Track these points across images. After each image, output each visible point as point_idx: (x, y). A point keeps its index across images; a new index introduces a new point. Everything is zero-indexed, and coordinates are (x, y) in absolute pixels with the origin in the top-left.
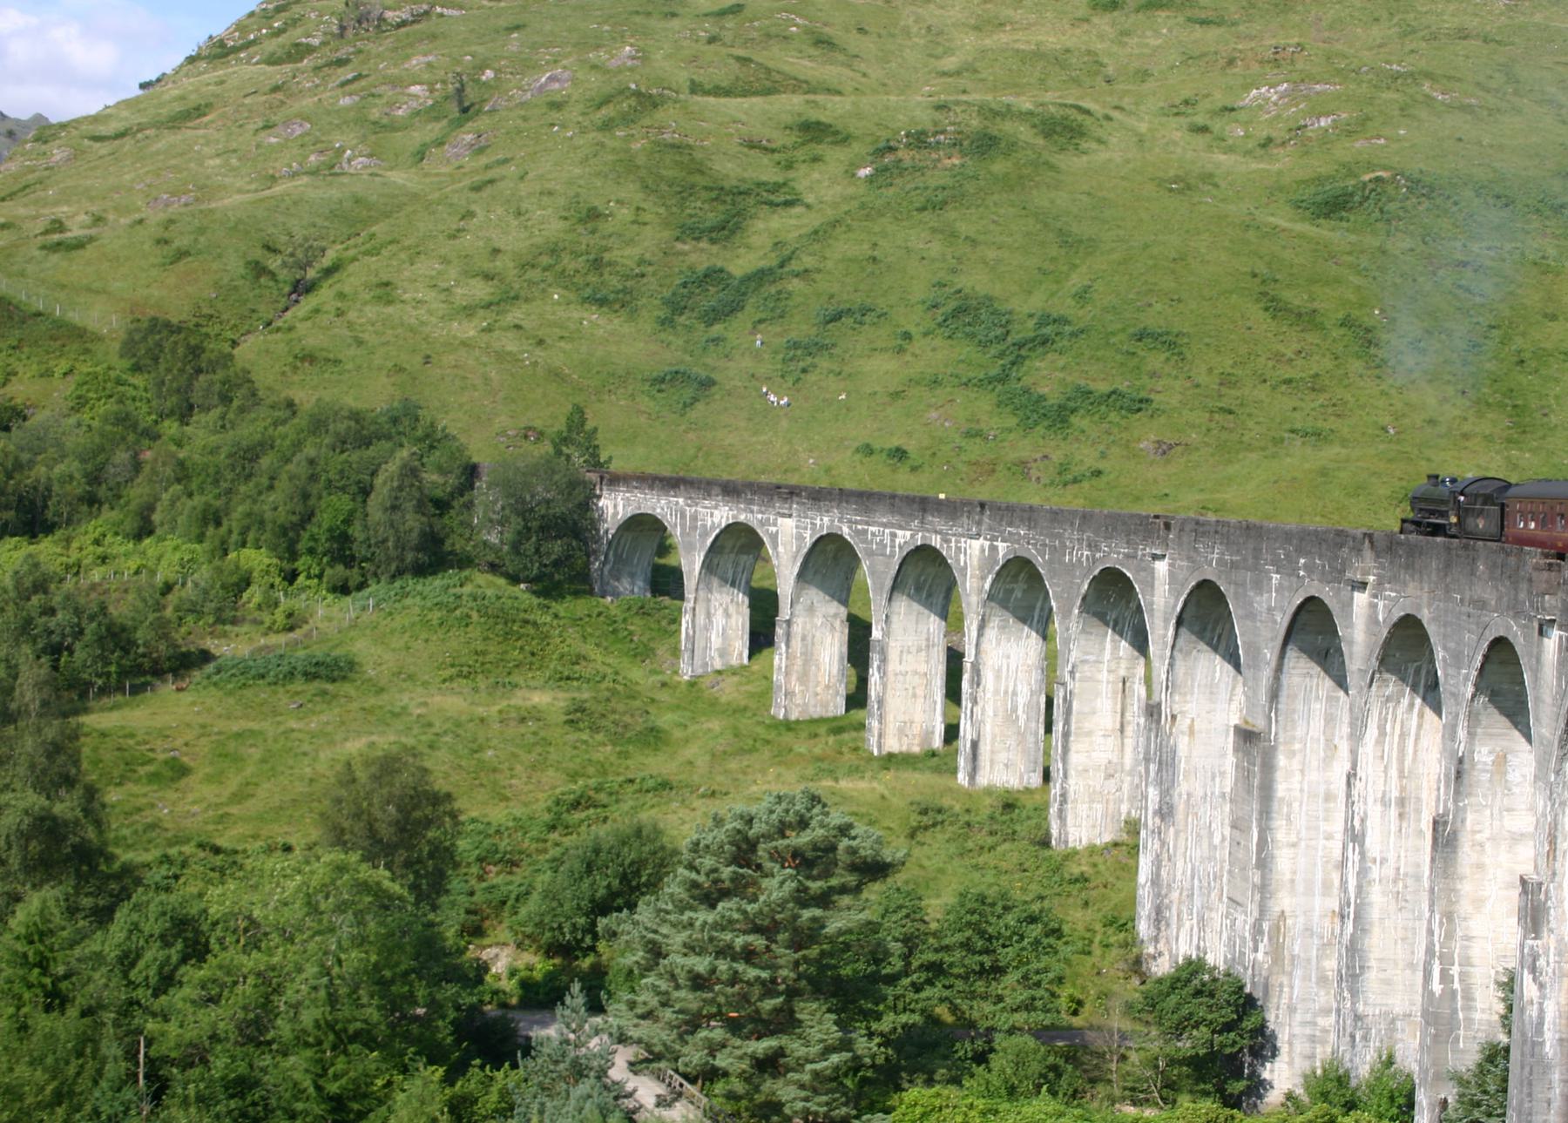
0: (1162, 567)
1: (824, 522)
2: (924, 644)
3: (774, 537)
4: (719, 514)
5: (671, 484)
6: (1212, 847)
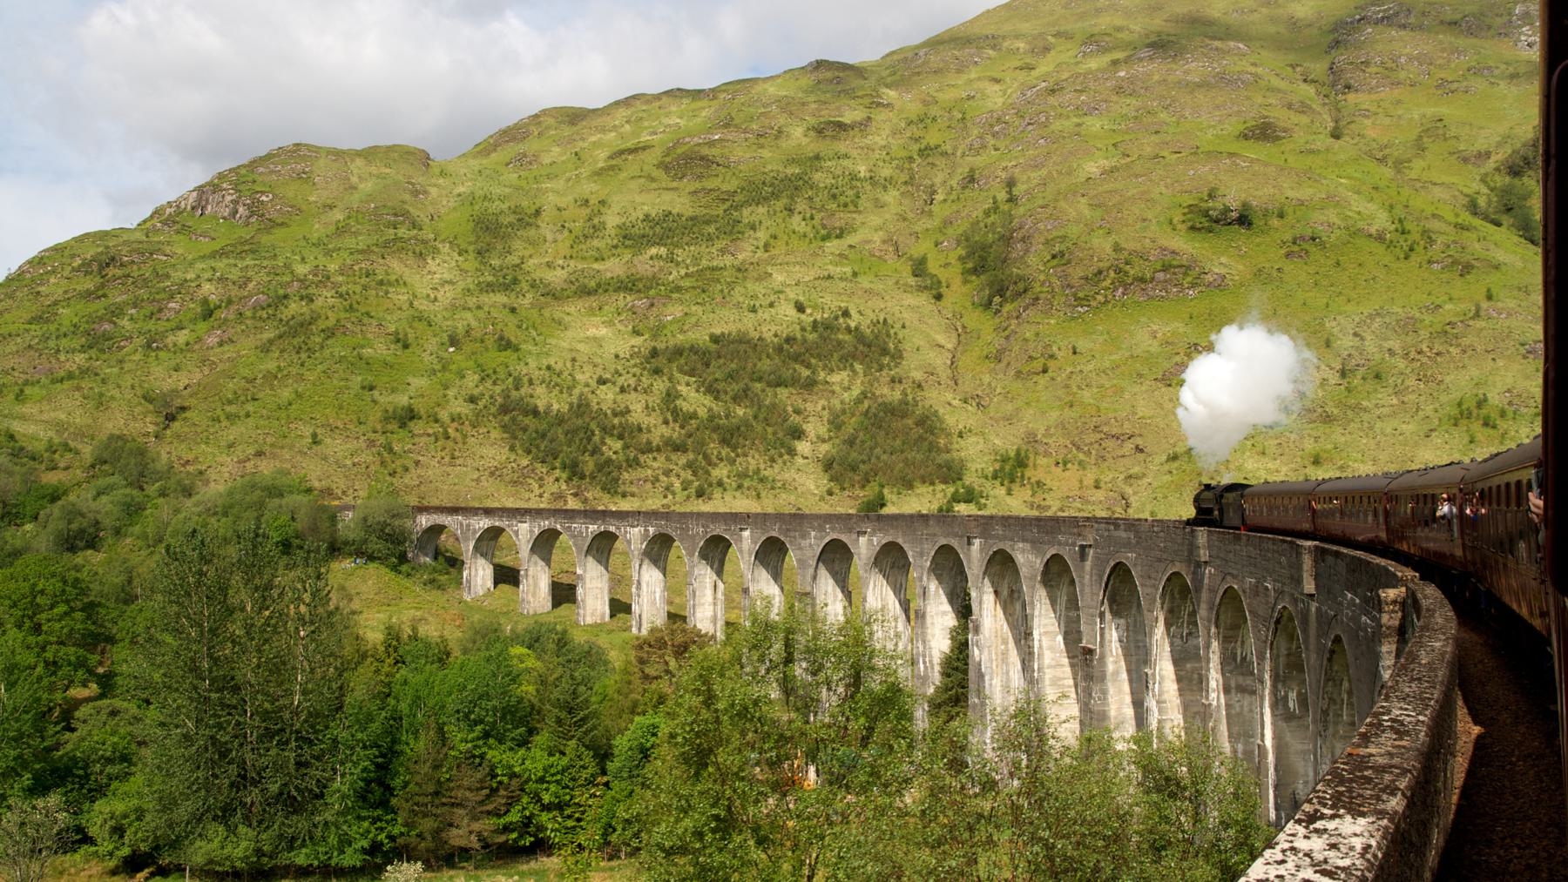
0: (746, 534)
1: (546, 524)
3: (517, 533)
4: (484, 523)
5: (454, 510)
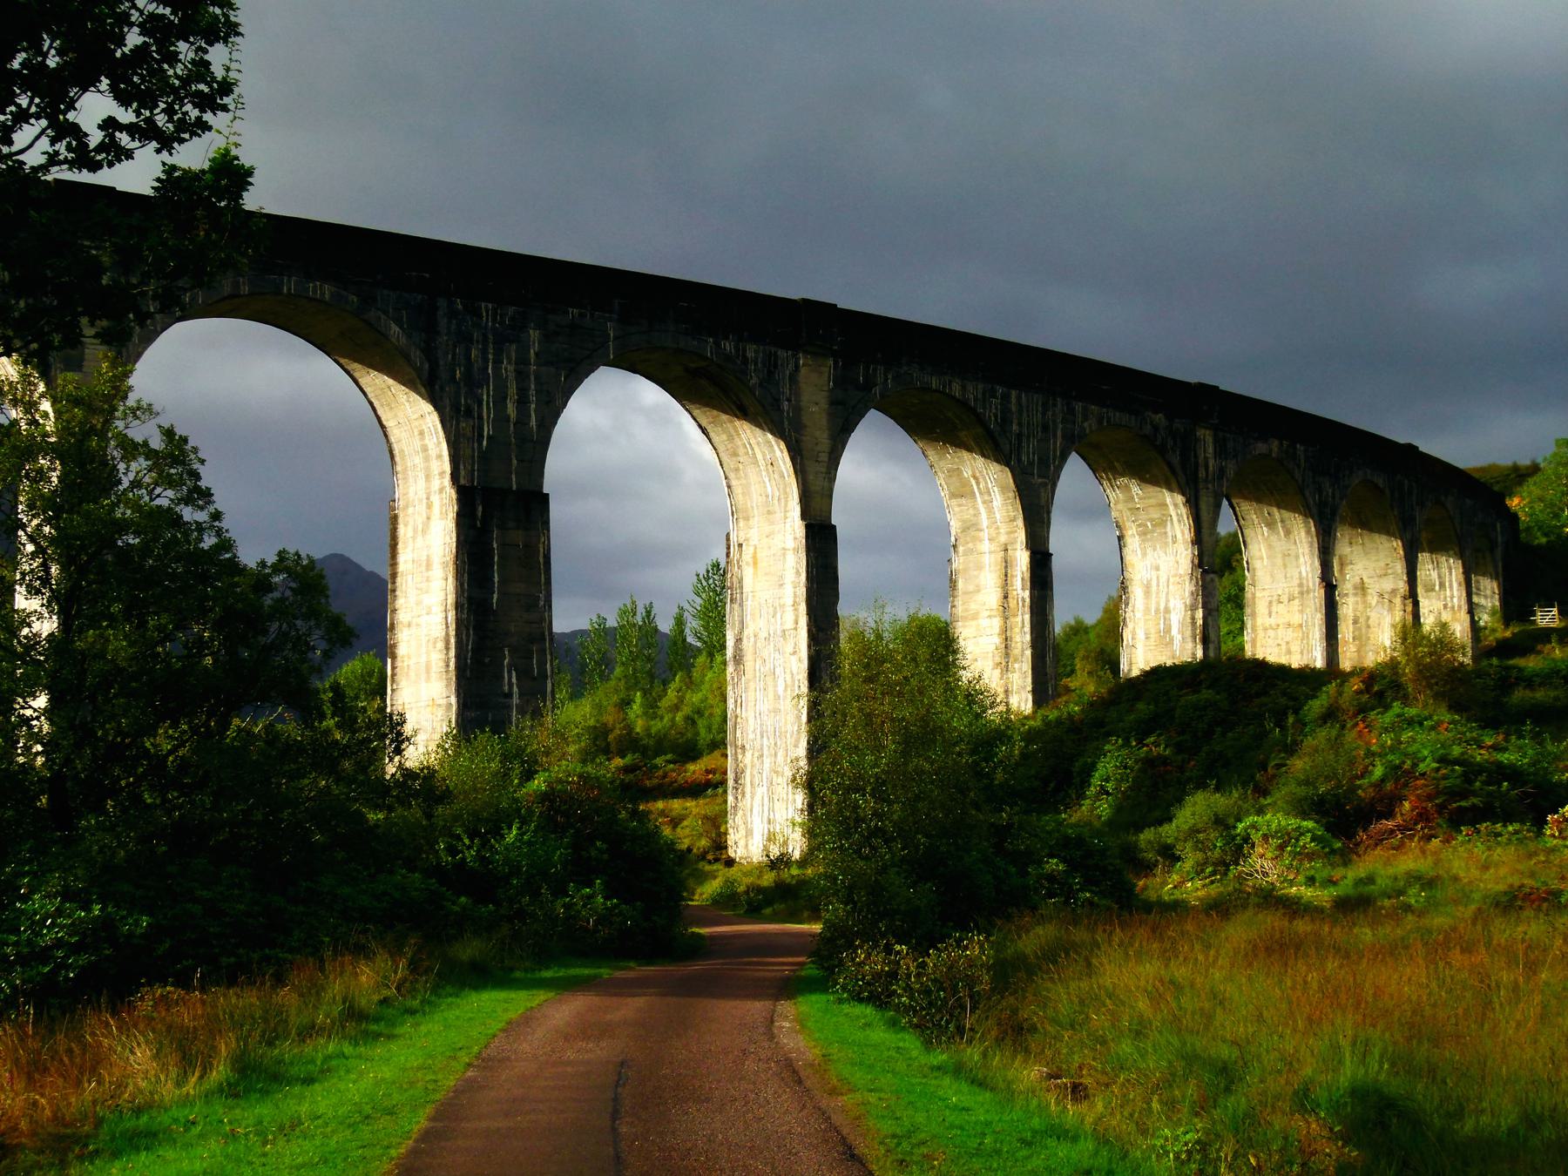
2: (1297, 590)
6: (777, 697)
